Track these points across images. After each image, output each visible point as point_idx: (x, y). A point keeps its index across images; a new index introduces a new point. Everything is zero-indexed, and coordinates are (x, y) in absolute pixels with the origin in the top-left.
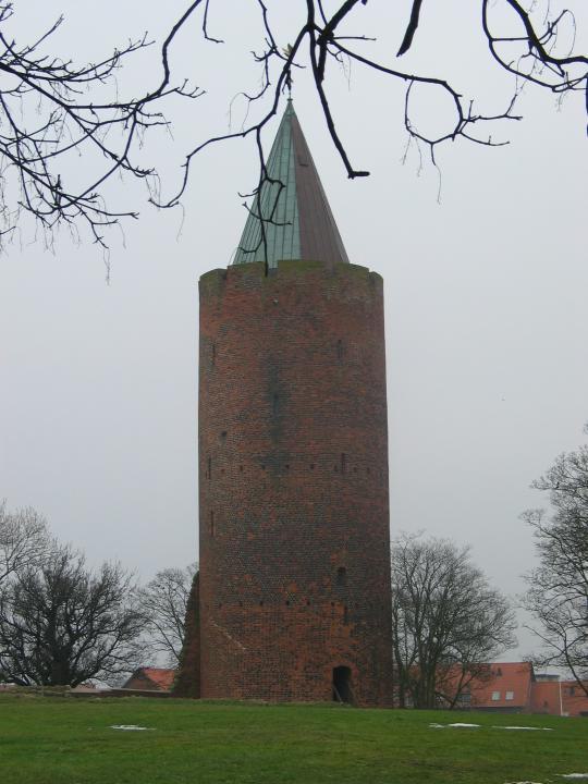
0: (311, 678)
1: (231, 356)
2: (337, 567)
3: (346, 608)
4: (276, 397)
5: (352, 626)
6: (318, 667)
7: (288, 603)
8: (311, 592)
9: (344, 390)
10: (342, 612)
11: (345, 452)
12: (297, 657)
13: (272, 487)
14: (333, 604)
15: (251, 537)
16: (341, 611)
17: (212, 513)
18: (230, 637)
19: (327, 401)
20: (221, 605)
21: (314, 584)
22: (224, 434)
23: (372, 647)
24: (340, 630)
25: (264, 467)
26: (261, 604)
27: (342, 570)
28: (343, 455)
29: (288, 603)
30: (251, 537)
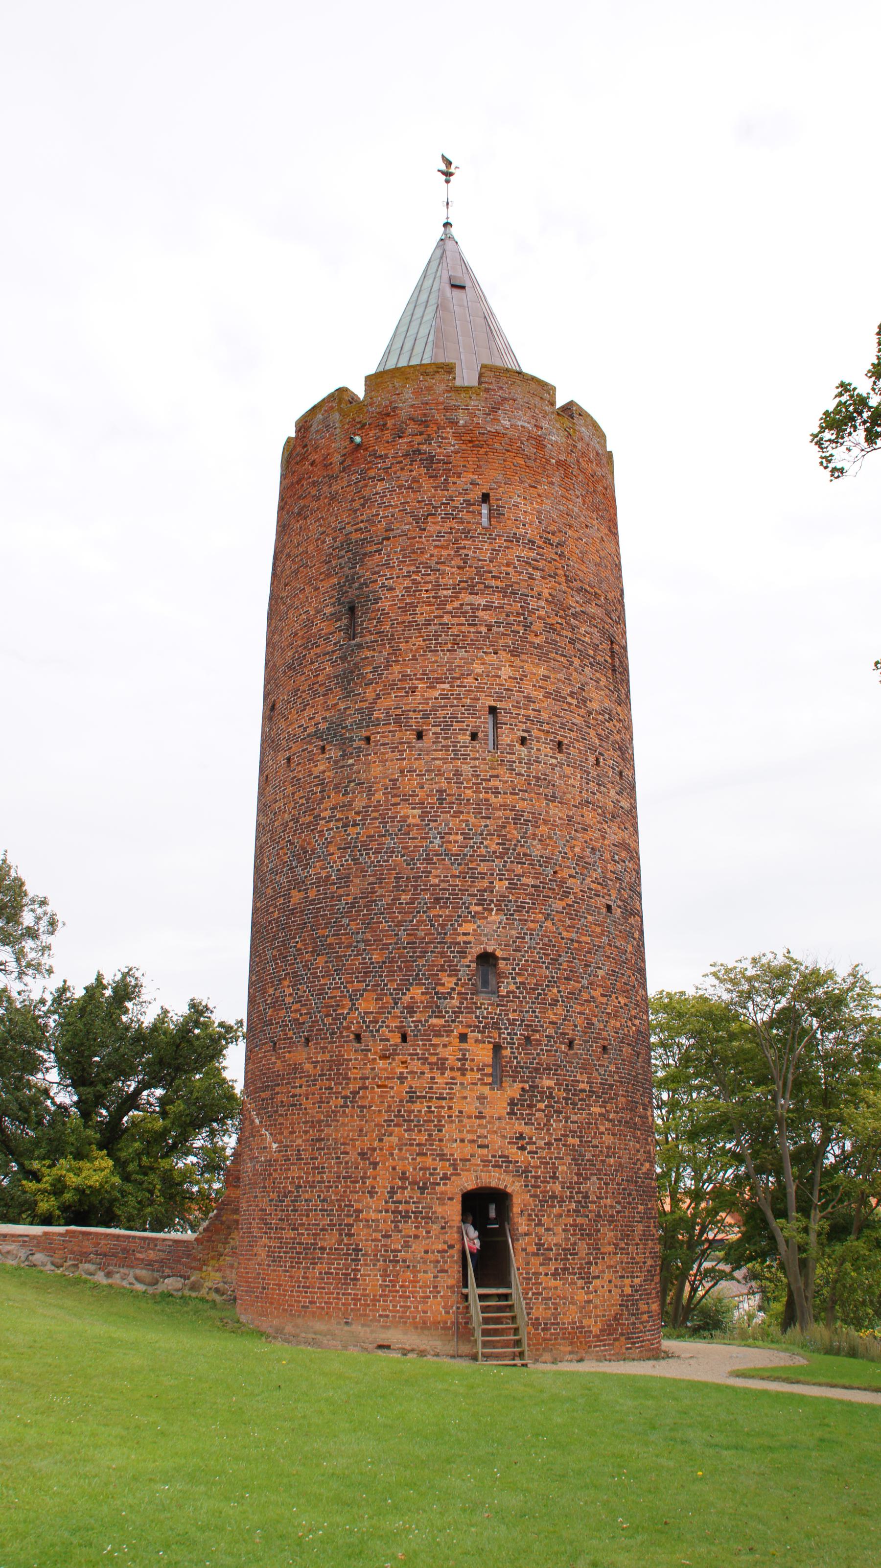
0: (406, 1217)
2: (475, 950)
3: (497, 1048)
4: (352, 610)
5: (513, 1090)
6: (422, 1189)
8: (411, 1009)
9: (493, 583)
10: (489, 1060)
11: (498, 705)
13: (336, 786)
14: (463, 1038)
15: (296, 897)
16: (482, 1054)
18: (257, 1121)
19: (456, 604)
21: (417, 992)
23: (573, 1141)
24: (482, 1098)
26: (307, 1040)
27: (487, 959)
28: (493, 710)
29: (358, 1038)
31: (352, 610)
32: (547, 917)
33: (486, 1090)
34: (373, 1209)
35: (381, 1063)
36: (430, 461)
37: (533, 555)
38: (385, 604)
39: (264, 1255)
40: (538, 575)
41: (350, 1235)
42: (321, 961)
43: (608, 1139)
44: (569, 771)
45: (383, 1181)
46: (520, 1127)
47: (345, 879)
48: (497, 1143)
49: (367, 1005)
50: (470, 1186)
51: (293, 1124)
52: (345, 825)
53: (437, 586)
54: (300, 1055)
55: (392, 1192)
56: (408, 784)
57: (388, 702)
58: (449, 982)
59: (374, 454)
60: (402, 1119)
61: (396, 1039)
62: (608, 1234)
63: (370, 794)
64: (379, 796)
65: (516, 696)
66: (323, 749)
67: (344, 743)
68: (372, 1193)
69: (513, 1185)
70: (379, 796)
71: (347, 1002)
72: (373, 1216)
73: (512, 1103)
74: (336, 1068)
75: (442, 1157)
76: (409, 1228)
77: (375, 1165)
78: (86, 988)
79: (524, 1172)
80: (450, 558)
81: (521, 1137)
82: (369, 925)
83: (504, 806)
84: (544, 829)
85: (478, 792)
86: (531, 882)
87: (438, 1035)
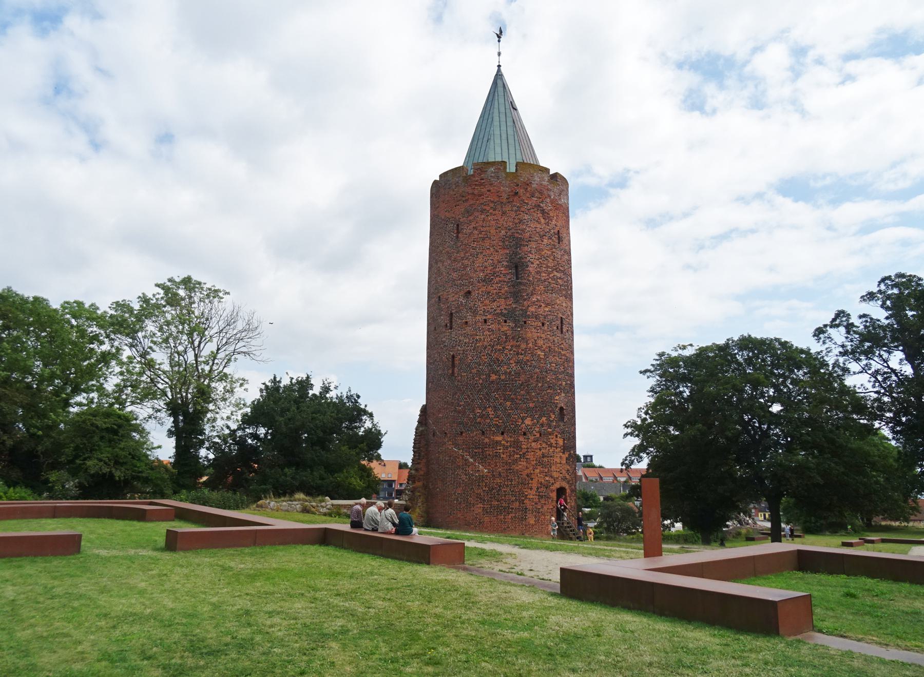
1: (476, 232)
2: (559, 406)
4: (516, 267)
7: (525, 434)
15: (494, 377)
16: (561, 442)
17: (453, 357)
20: (462, 433)
21: (544, 419)
26: (502, 434)
27: (561, 409)
29: (525, 434)
30: (494, 377)
31: (516, 267)
34: (532, 494)
35: (533, 444)
36: (543, 212)
38: (532, 269)
39: (480, 511)
42: (508, 404)
45: (534, 485)
47: (518, 374)
48: (564, 472)
49: (528, 421)
51: (496, 463)
52: (518, 354)
53: (548, 267)
54: (499, 438)
56: (540, 342)
57: (532, 309)
58: (553, 416)
59: (523, 201)
60: (540, 463)
61: (538, 435)
66: (505, 322)
67: (516, 321)
68: (531, 489)
69: (567, 487)
70: (530, 345)
71: (520, 420)
74: (517, 445)
75: (552, 477)
76: (543, 501)
79: (568, 482)
82: (528, 393)
83: (564, 355)
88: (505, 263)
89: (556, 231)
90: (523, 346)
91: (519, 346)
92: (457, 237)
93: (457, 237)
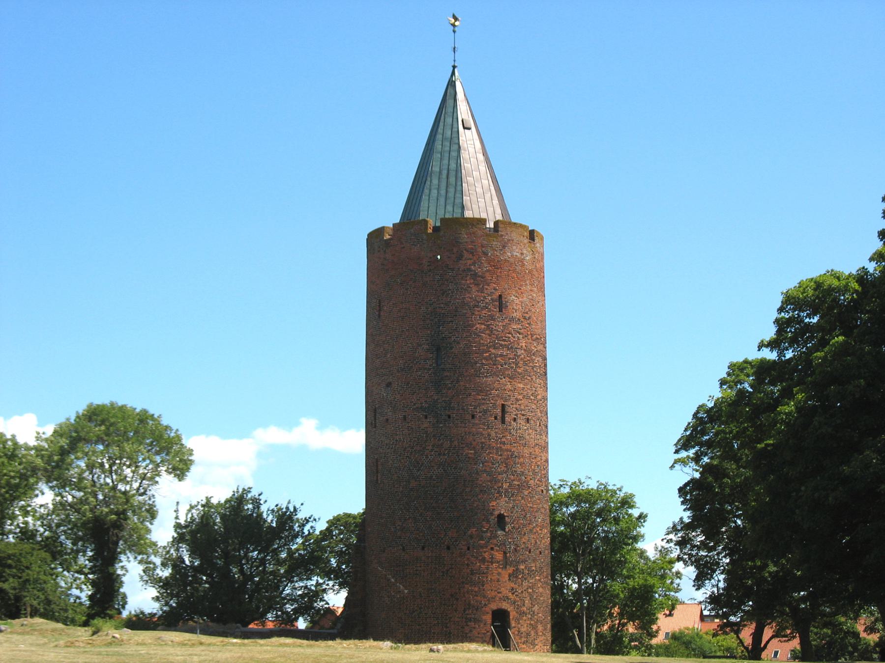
2: (496, 513)
3: (505, 553)
4: (438, 350)
5: (510, 570)
12: (457, 599)
13: (434, 436)
14: (492, 549)
17: (377, 461)
18: (393, 580)
22: (389, 385)
23: (530, 590)
25: (426, 417)
26: (423, 548)
27: (501, 517)
29: (448, 548)
31: (438, 350)
32: (523, 498)
33: (500, 570)
37: (519, 326)
40: (521, 336)
41: (446, 627)
43: (541, 590)
44: (531, 431)
46: (513, 585)
50: (495, 608)
55: (464, 611)
62: (540, 627)
63: (451, 442)
64: (456, 443)
65: (512, 399)
68: (456, 611)
70: (456, 443)
72: (457, 619)
73: (510, 576)
75: (484, 597)
77: (457, 599)
78: (328, 522)
80: (484, 330)
81: (513, 589)
84: (522, 460)
85: (497, 444)
86: (517, 483)
87: (482, 547)
88: (426, 347)
89: (496, 296)
90: (447, 444)
91: (442, 444)
92: (379, 316)
93: (379, 316)
